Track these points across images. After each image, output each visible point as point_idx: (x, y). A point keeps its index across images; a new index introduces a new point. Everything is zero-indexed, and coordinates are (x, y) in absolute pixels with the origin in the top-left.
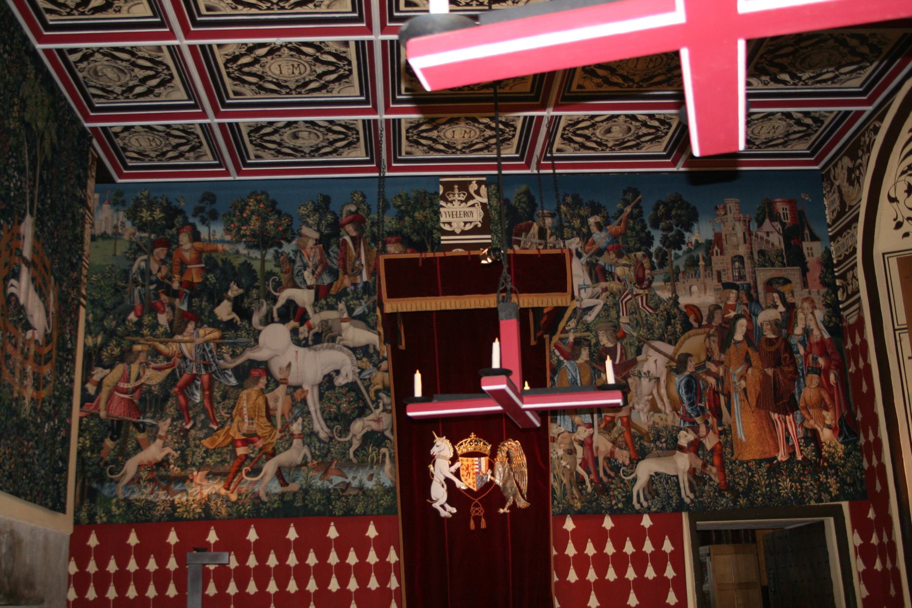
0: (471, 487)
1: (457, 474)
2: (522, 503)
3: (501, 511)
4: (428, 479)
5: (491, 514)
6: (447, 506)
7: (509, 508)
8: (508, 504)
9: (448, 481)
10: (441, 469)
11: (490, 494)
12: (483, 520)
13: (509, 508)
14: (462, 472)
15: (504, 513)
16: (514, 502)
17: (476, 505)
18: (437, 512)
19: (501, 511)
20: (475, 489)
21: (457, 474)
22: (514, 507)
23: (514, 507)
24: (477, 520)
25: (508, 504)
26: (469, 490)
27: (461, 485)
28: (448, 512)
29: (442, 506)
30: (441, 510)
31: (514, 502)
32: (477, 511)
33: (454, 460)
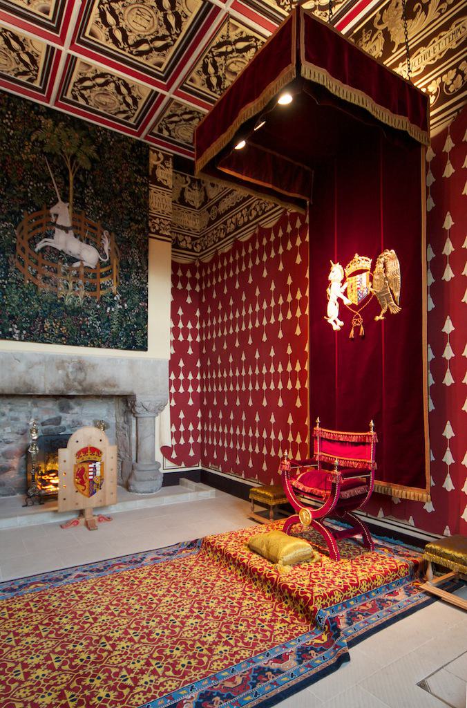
0: (354, 302)
1: (345, 294)
2: (396, 310)
3: (377, 318)
4: (325, 301)
5: (369, 322)
6: (338, 320)
7: (384, 315)
8: (384, 311)
9: (340, 300)
10: (334, 292)
11: (370, 304)
12: (362, 328)
13: (384, 315)
14: (349, 291)
15: (380, 320)
16: (388, 309)
17: (357, 317)
18: (330, 326)
19: (377, 318)
20: (356, 304)
21: (345, 294)
22: (388, 314)
23: (388, 314)
24: (357, 329)
25: (384, 311)
26: (353, 306)
27: (347, 302)
28: (337, 325)
29: (335, 321)
30: (333, 324)
31: (388, 309)
32: (358, 321)
33: (343, 282)
